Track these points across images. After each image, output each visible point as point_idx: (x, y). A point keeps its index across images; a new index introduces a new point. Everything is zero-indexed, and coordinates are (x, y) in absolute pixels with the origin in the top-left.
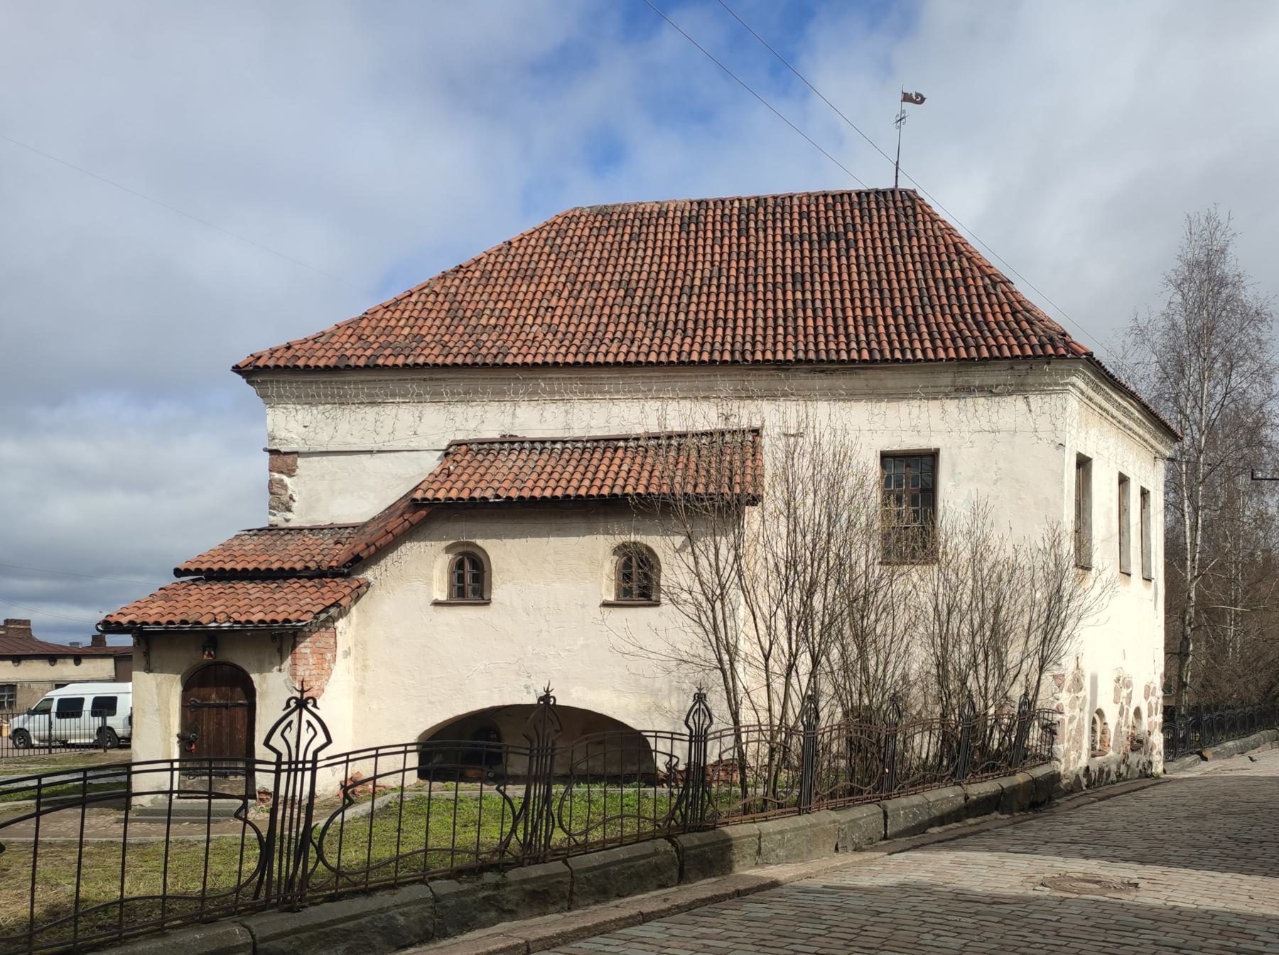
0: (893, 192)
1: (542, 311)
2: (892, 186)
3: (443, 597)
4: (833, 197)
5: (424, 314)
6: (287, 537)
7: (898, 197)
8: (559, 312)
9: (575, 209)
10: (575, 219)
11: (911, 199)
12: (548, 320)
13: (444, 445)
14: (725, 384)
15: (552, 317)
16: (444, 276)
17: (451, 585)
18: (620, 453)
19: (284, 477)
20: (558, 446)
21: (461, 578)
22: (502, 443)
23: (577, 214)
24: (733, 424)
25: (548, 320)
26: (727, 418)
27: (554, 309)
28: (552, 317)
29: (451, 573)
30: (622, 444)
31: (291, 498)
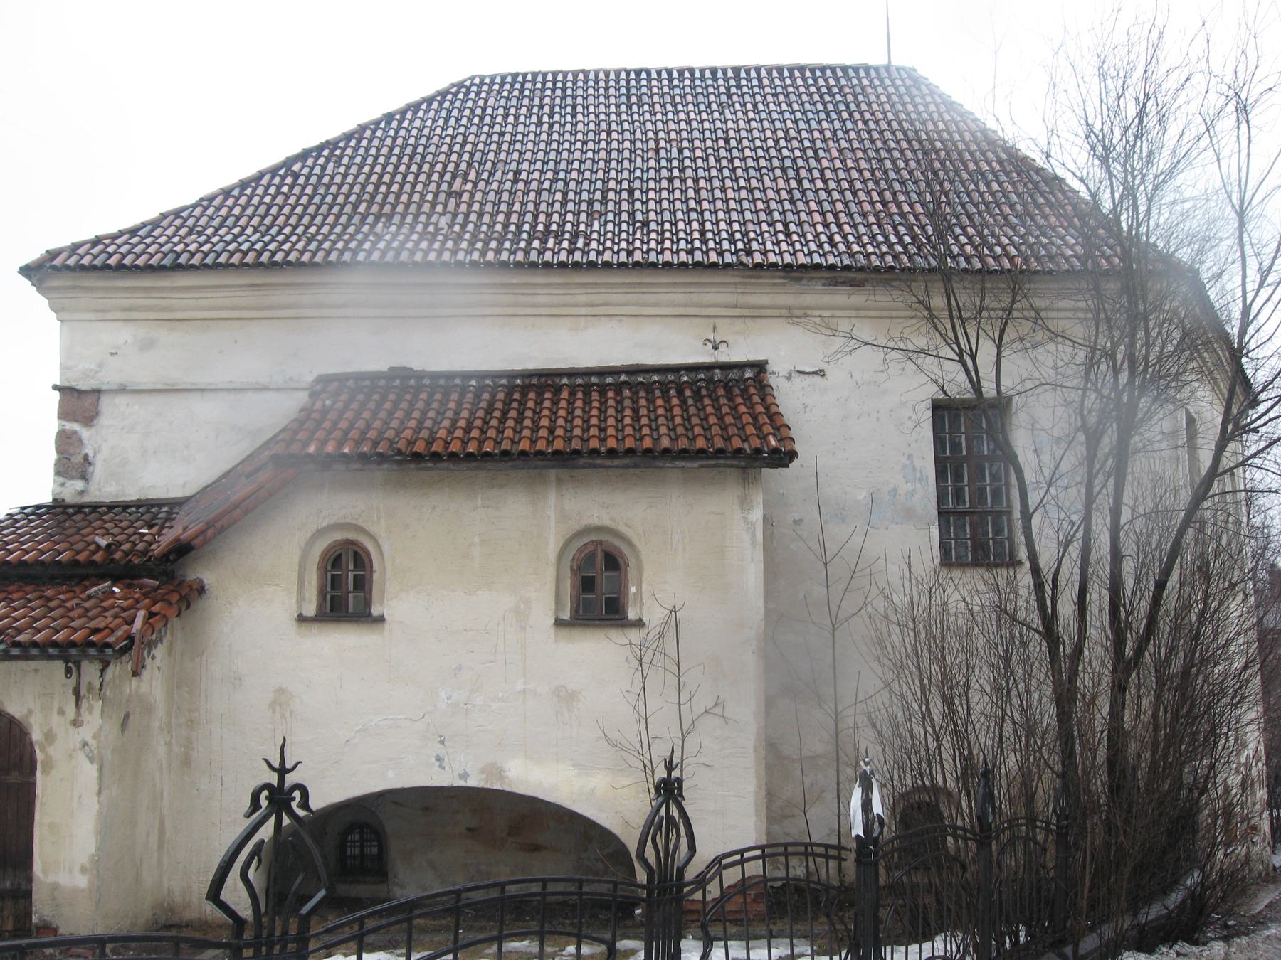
0: (887, 68)
1: (442, 197)
2: (885, 62)
3: (310, 609)
4: (813, 71)
5: (280, 200)
6: (78, 517)
7: (895, 74)
8: (466, 197)
9: (473, 78)
10: (474, 89)
11: (910, 77)
12: (451, 207)
13: (309, 378)
14: (716, 294)
15: (458, 206)
16: (304, 155)
17: (322, 593)
18: (565, 394)
19: (76, 427)
20: (473, 383)
21: (336, 582)
22: (394, 378)
23: (477, 81)
24: (725, 356)
25: (451, 207)
26: (715, 348)
27: (460, 194)
28: (458, 206)
29: (323, 569)
30: (565, 381)
31: (86, 457)
